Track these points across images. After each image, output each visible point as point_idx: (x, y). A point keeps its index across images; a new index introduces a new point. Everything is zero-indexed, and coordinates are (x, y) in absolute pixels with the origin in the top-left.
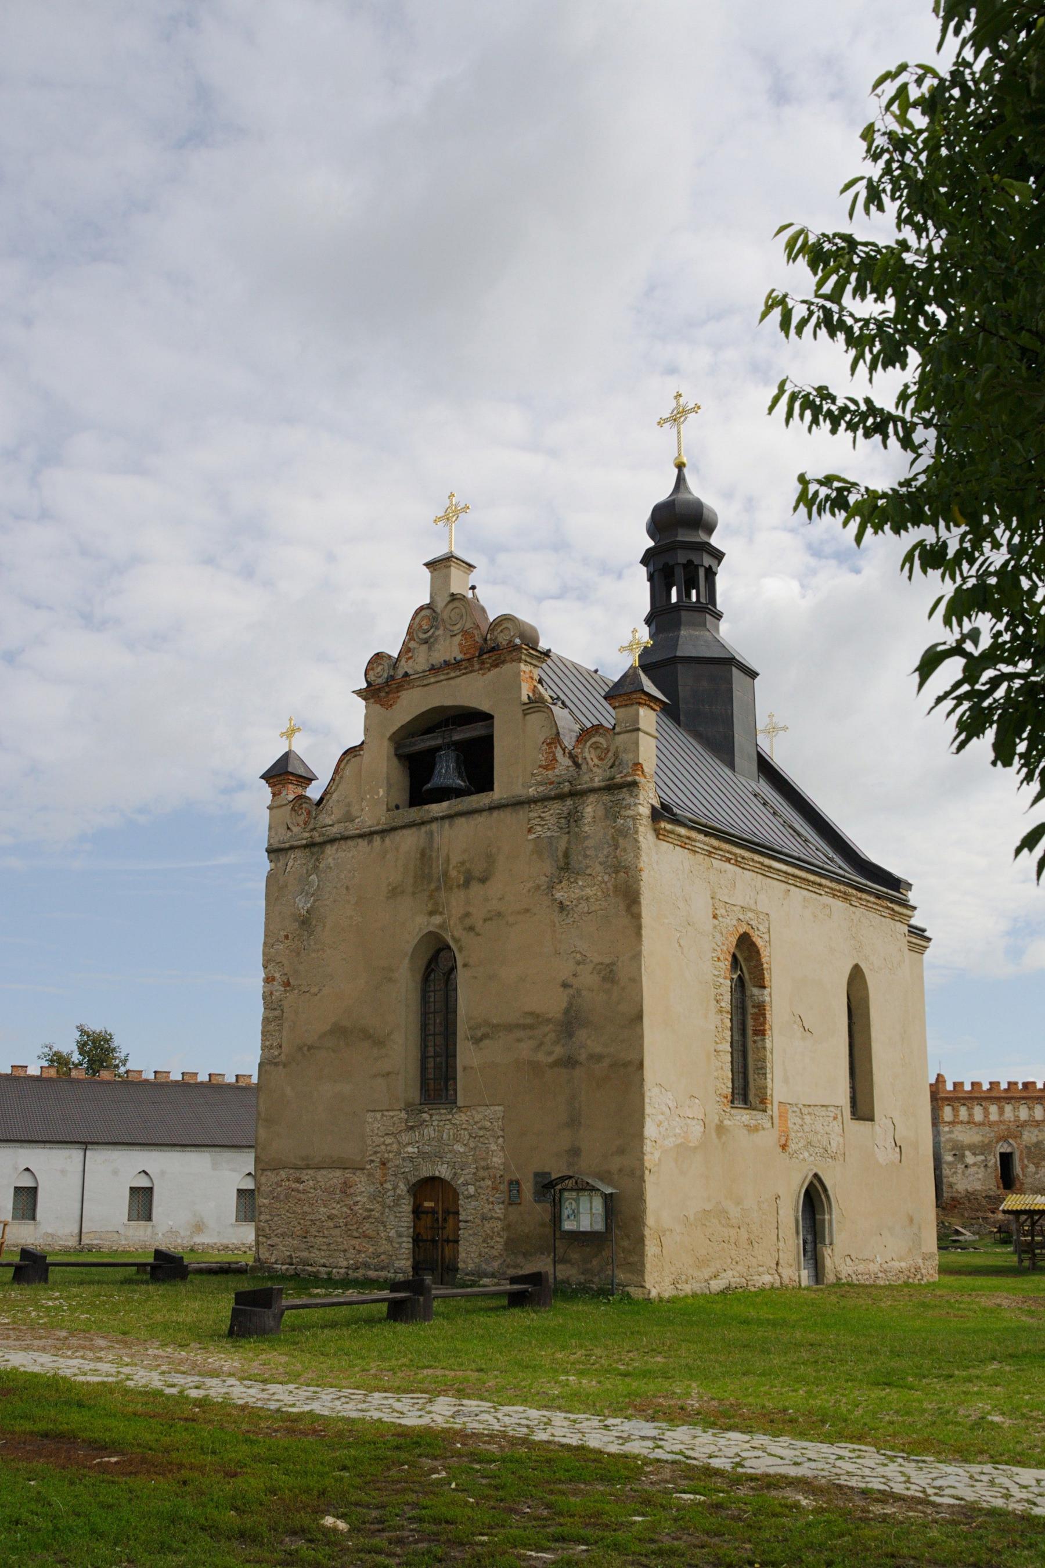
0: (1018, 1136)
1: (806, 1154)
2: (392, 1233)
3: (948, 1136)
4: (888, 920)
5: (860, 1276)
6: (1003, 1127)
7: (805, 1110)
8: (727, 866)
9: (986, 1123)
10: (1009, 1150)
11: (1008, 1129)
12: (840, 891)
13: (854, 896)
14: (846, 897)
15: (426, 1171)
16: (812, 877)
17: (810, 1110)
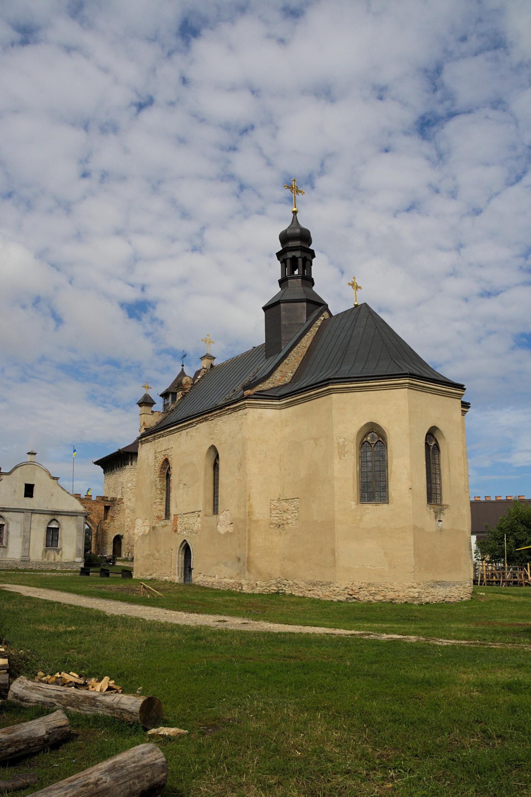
1: (185, 533)
4: (232, 414)
5: (204, 583)
7: (185, 516)
8: (161, 439)
12: (201, 419)
13: (208, 417)
14: (206, 420)
16: (186, 423)
17: (186, 515)
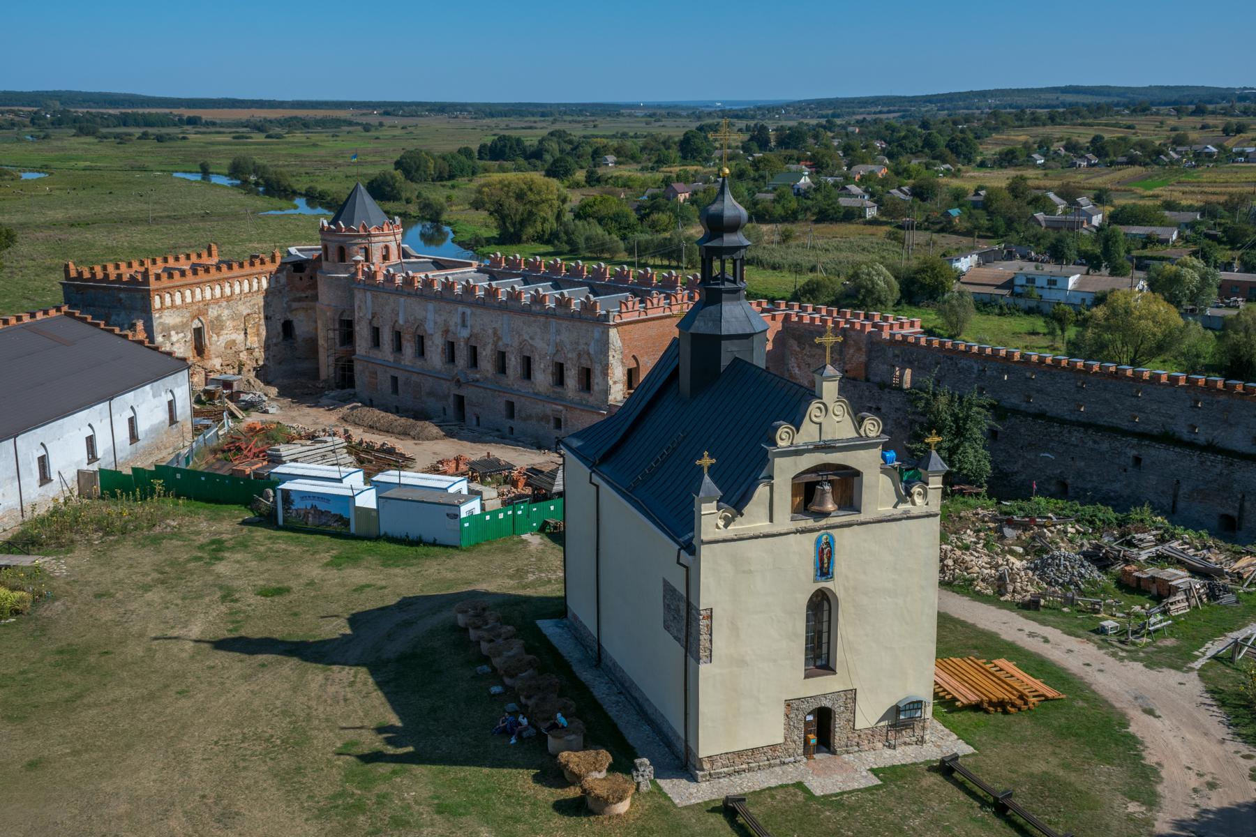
0: (205, 313)
2: (796, 738)
3: (159, 321)
6: (195, 308)
9: (185, 305)
10: (200, 325)
11: (199, 309)
15: (815, 705)
